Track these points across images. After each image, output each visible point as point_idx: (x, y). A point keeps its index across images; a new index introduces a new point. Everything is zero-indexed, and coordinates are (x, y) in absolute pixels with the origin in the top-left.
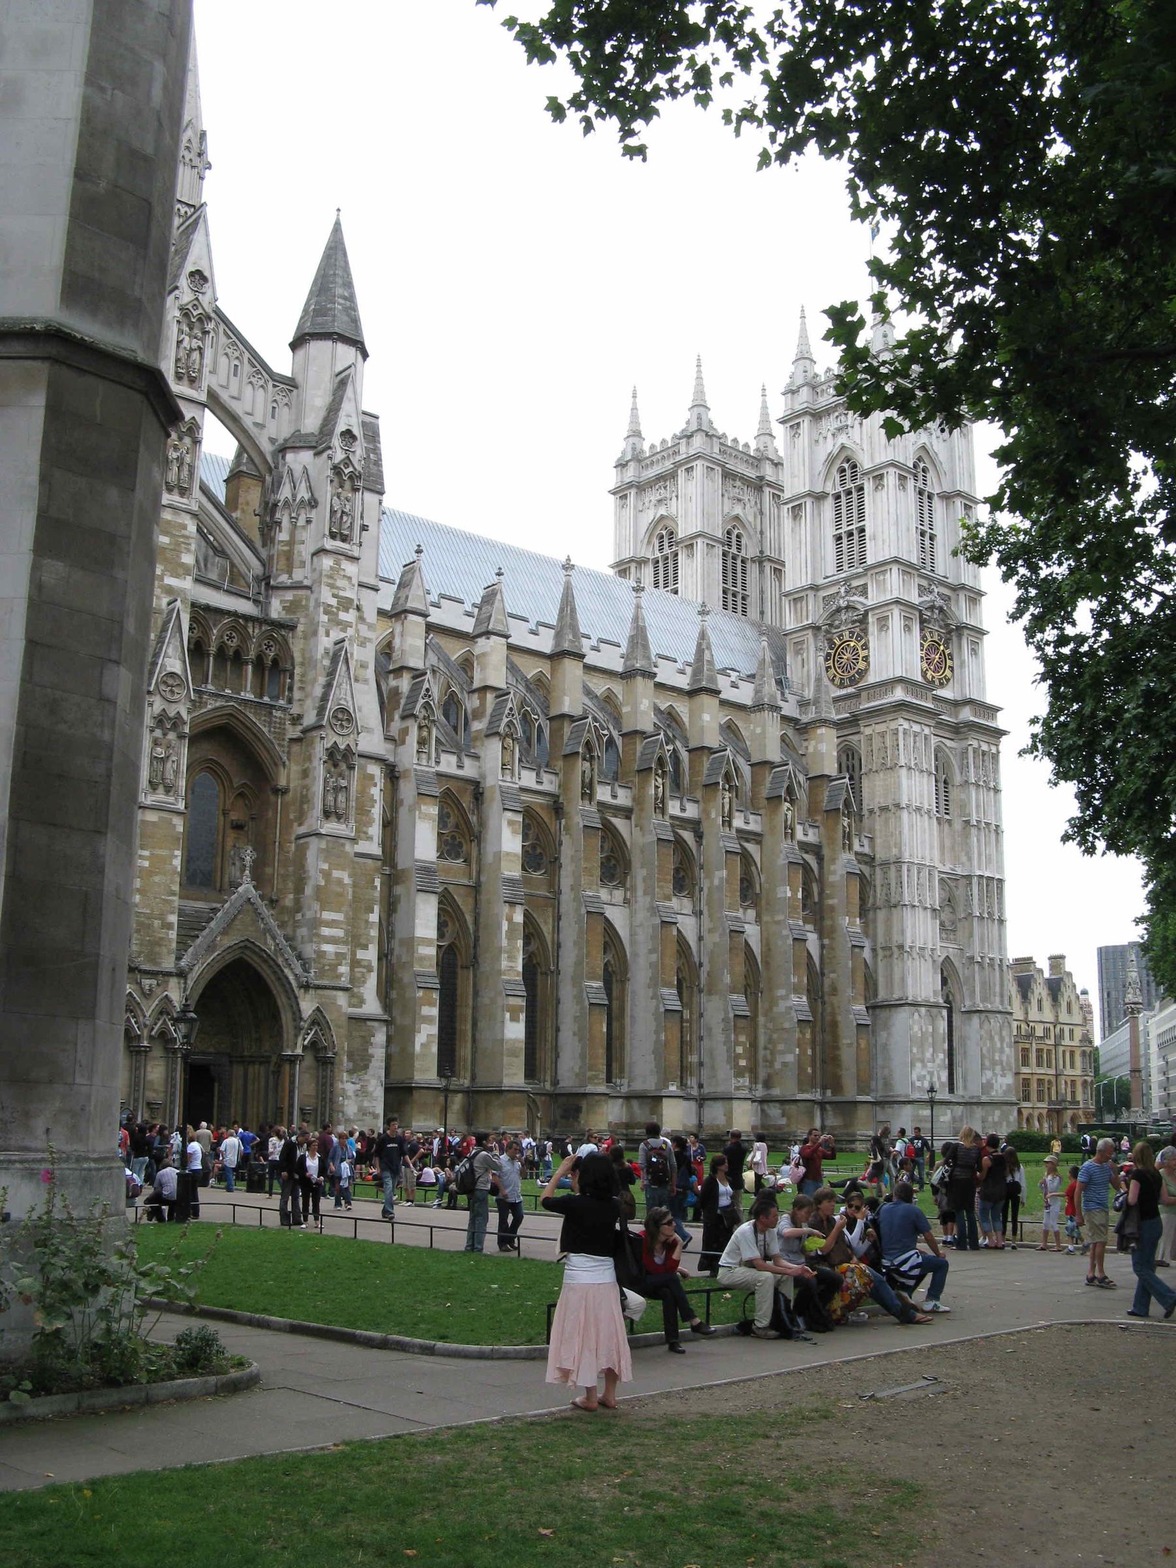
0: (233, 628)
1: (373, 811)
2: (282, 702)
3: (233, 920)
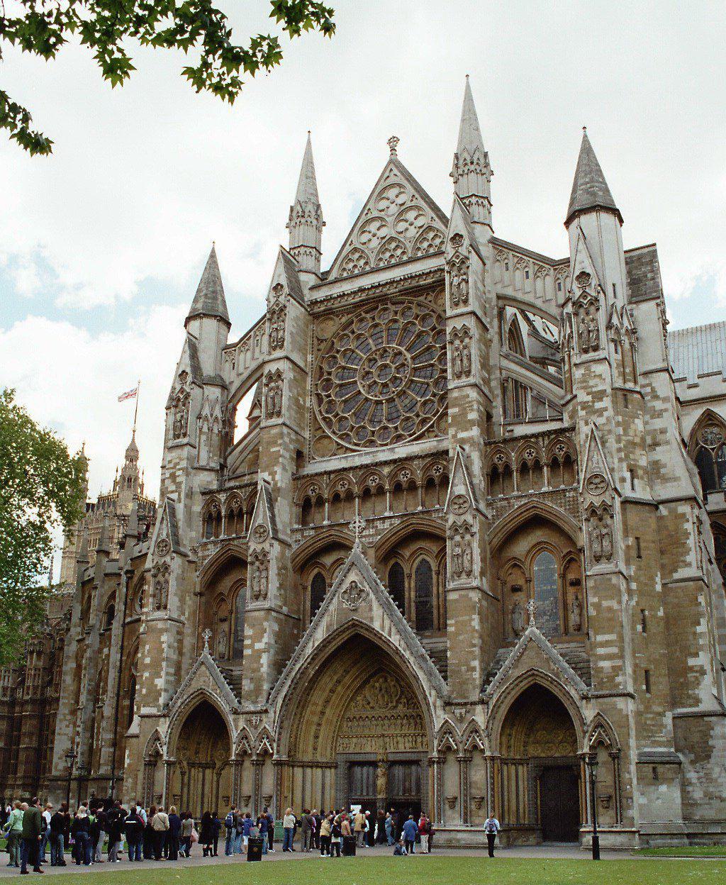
1: (688, 541)
2: (575, 485)
3: (521, 656)
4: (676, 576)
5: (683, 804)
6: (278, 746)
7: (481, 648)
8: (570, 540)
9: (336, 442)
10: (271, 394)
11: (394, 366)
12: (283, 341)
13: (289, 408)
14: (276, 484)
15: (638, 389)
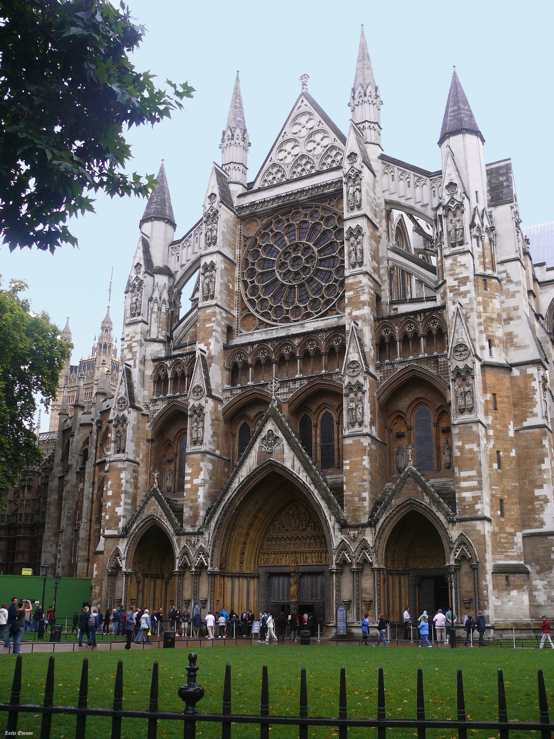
0: (409, 322)
1: (535, 396)
2: (445, 352)
3: (401, 489)
4: (525, 424)
5: (530, 605)
6: (212, 560)
7: (370, 482)
8: (442, 397)
9: (259, 319)
10: (207, 281)
11: (304, 258)
12: (216, 239)
13: (221, 292)
14: (210, 353)
15: (495, 275)
